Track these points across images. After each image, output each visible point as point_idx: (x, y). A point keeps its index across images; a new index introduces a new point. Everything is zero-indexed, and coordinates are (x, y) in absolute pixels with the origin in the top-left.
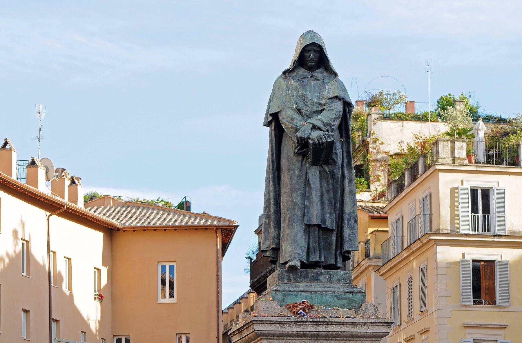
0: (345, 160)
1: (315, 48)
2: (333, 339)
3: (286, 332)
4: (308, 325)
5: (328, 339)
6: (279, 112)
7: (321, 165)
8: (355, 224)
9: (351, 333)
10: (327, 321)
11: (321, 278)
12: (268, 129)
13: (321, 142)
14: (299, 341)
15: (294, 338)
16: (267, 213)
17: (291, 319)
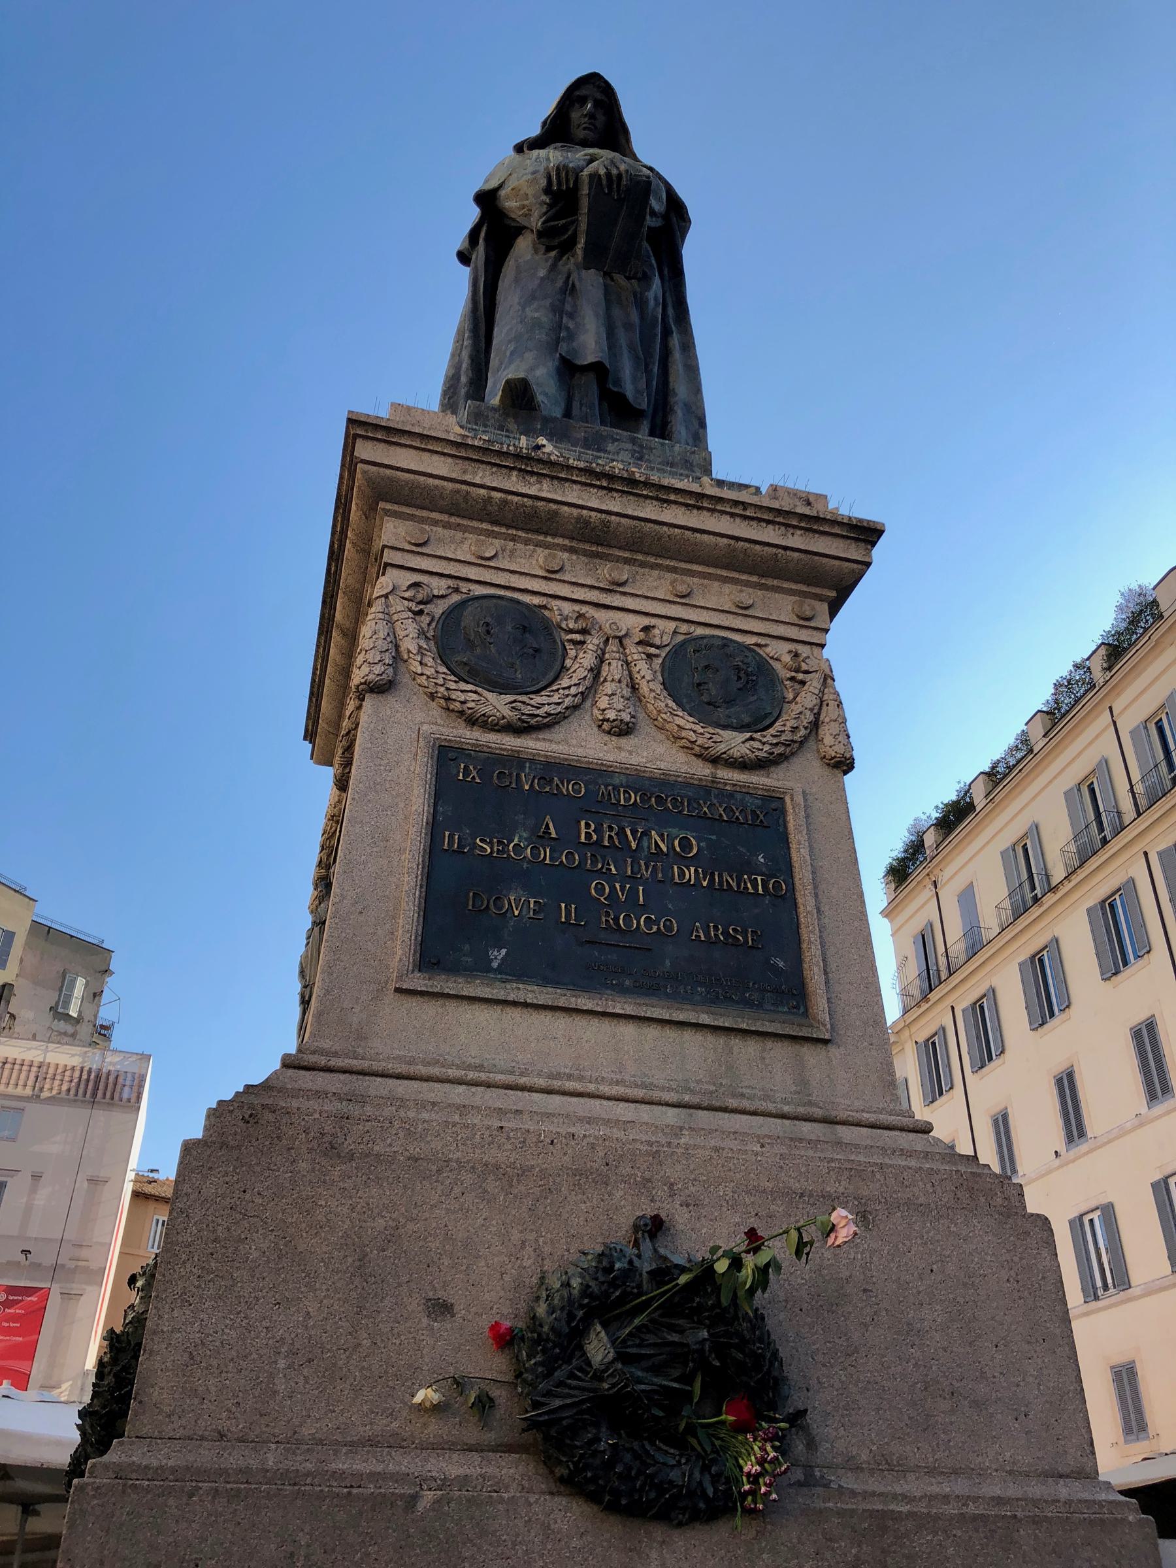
0: (670, 311)
1: (599, 96)
2: (659, 561)
3: (482, 492)
4: (567, 485)
5: (640, 557)
6: (501, 186)
7: (607, 274)
8: (701, 431)
9: (725, 541)
10: (642, 479)
11: (610, 447)
12: (465, 272)
13: (614, 172)
14: (532, 547)
15: (510, 532)
16: (449, 398)
17: (505, 446)
